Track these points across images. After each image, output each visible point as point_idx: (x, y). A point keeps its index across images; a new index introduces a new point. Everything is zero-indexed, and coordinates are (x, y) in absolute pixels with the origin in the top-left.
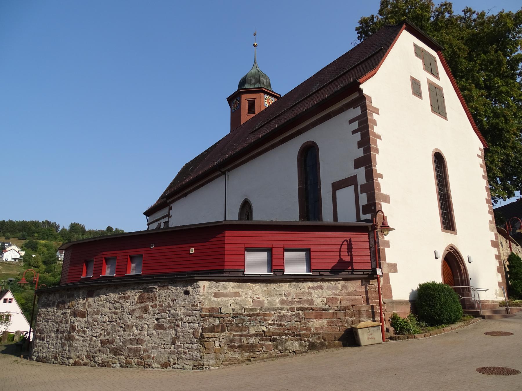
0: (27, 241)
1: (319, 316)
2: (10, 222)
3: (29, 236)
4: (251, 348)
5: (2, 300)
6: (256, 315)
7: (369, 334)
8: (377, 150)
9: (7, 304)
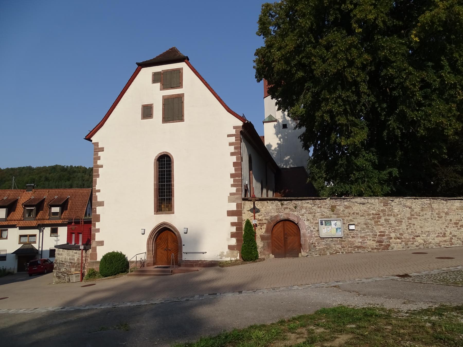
8: (98, 176)
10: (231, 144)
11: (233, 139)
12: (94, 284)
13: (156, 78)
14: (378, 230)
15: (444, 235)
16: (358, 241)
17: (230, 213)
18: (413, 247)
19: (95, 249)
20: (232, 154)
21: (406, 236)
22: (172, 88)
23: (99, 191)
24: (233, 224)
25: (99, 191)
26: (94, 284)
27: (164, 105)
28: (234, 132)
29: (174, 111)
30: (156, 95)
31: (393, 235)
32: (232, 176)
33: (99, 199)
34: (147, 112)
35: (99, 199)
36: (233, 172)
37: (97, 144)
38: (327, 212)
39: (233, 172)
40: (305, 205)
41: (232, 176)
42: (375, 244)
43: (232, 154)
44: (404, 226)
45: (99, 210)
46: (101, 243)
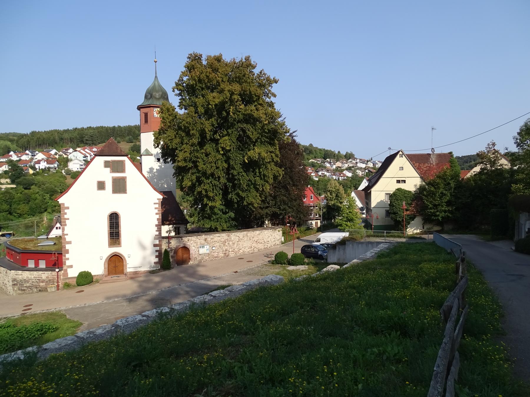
0: (133, 144)
1: (43, 282)
2: (119, 127)
3: (134, 139)
4: (24, 290)
5: (55, 228)
6: (26, 281)
7: (52, 289)
9: (58, 230)
10: (156, 208)
11: (157, 206)
12: (83, 291)
13: (107, 164)
14: (224, 248)
15: (251, 248)
16: (215, 254)
17: (155, 245)
18: (238, 254)
19: (66, 270)
20: (157, 214)
21: (236, 250)
22: (118, 172)
23: (67, 235)
24: (157, 251)
25: (67, 235)
26: (83, 291)
27: (113, 182)
28: (157, 201)
29: (120, 186)
30: (108, 176)
31: (231, 250)
32: (156, 226)
33: (67, 240)
34: (101, 186)
35: (67, 240)
36: (157, 223)
37: (64, 204)
38: (203, 242)
39: (157, 223)
40: (193, 239)
41: (156, 226)
42: (223, 255)
43: (157, 214)
44: (235, 245)
45: (68, 247)
46: (71, 267)
